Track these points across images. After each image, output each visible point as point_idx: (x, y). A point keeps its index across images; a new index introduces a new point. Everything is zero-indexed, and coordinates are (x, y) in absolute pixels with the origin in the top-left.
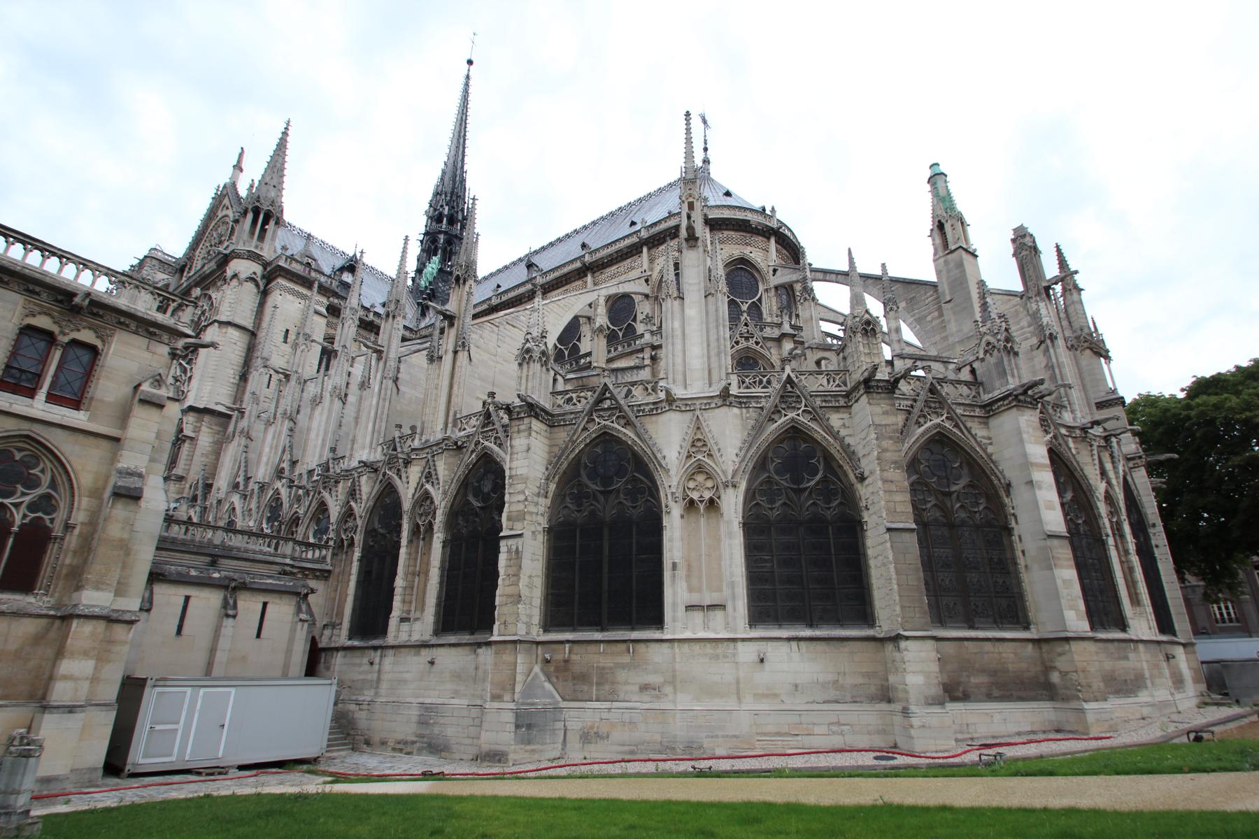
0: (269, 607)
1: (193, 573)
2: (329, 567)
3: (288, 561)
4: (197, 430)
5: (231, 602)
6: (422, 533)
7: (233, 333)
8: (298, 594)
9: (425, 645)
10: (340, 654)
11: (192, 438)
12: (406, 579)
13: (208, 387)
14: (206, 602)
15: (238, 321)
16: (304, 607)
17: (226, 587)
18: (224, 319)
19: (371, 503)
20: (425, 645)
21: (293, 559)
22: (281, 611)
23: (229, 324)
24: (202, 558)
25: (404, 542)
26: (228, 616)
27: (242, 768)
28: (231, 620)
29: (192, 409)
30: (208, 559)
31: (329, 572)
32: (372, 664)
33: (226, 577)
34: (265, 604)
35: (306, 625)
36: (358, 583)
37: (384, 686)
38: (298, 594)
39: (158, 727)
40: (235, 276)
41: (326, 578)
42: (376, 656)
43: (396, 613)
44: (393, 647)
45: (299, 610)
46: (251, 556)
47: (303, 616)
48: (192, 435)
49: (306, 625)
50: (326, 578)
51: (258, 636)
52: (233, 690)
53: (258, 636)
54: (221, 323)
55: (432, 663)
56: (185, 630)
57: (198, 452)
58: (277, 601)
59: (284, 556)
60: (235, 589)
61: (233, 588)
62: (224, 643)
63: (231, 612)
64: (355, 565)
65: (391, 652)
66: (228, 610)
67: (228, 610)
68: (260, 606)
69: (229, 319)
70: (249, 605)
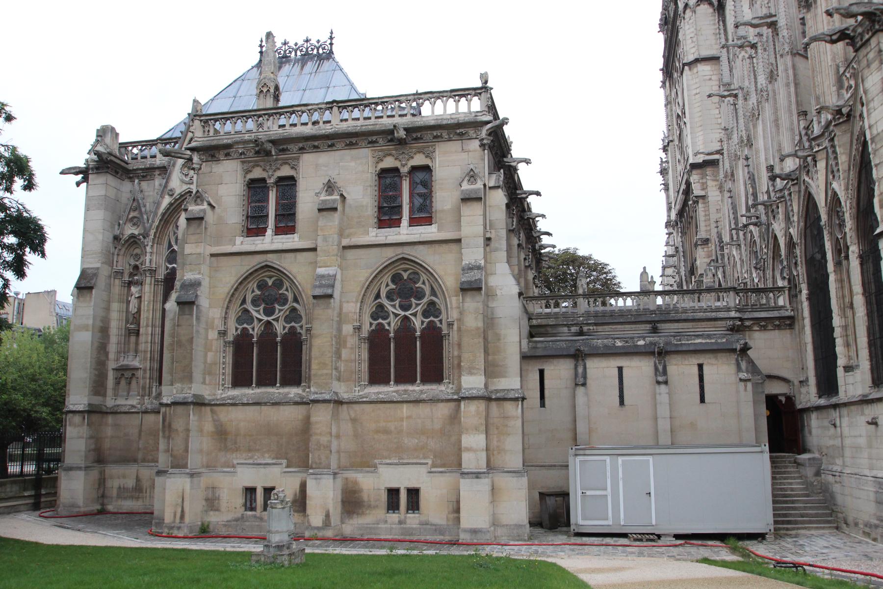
0: (706, 369)
1: (619, 344)
2: (789, 313)
3: (733, 314)
4: (704, 187)
5: (660, 368)
6: (841, 251)
7: (704, 69)
8: (734, 351)
9: (865, 401)
10: (814, 416)
11: (703, 197)
12: (844, 315)
13: (700, 140)
14: (639, 370)
15: (705, 53)
16: (744, 365)
17: (652, 353)
18: (691, 58)
19: (802, 224)
20: (865, 401)
21: (738, 310)
22: (721, 373)
23: (697, 61)
24: (643, 326)
25: (830, 267)
26: (658, 383)
27: (677, 537)
28: (663, 387)
29: (694, 166)
30: (648, 326)
31: (792, 318)
32: (835, 425)
33: (651, 343)
34: (700, 367)
35: (749, 385)
36: (813, 326)
37: (848, 453)
38: (734, 351)
39: (588, 493)
40: (686, 6)
41: (791, 326)
42: (834, 414)
43: (841, 362)
44: (845, 405)
45: (739, 369)
46: (690, 315)
47: (743, 375)
48: (702, 193)
49: (749, 385)
50: (791, 326)
51: (702, 400)
52: (650, 458)
53: (702, 400)
54: (690, 64)
55: (874, 423)
56: (626, 402)
57: (712, 210)
58: (713, 361)
59: (728, 309)
60: (660, 354)
61: (661, 354)
62: (664, 411)
63: (660, 379)
64: (806, 305)
65: (845, 411)
66: (662, 378)
67: (662, 378)
68: (696, 370)
69: (696, 56)
70: (682, 370)
